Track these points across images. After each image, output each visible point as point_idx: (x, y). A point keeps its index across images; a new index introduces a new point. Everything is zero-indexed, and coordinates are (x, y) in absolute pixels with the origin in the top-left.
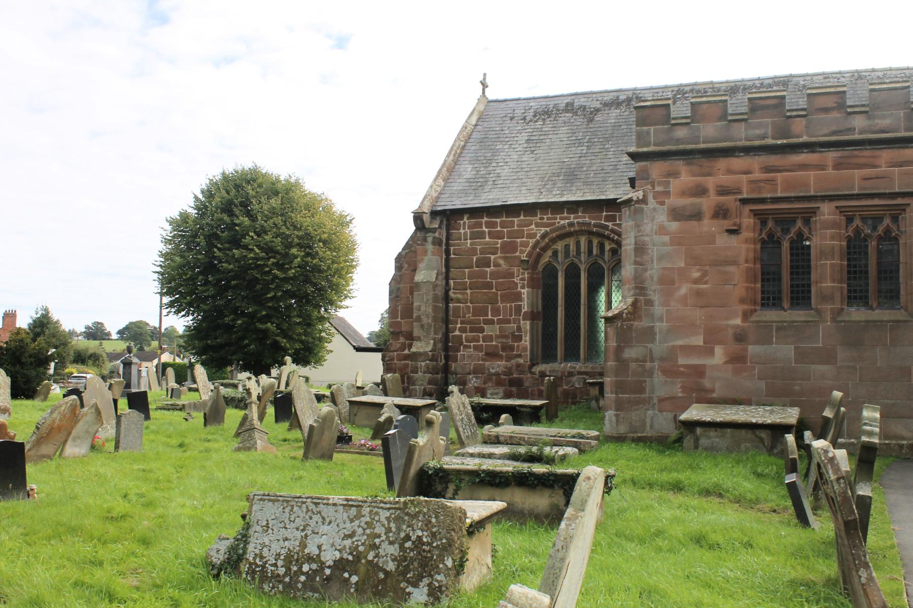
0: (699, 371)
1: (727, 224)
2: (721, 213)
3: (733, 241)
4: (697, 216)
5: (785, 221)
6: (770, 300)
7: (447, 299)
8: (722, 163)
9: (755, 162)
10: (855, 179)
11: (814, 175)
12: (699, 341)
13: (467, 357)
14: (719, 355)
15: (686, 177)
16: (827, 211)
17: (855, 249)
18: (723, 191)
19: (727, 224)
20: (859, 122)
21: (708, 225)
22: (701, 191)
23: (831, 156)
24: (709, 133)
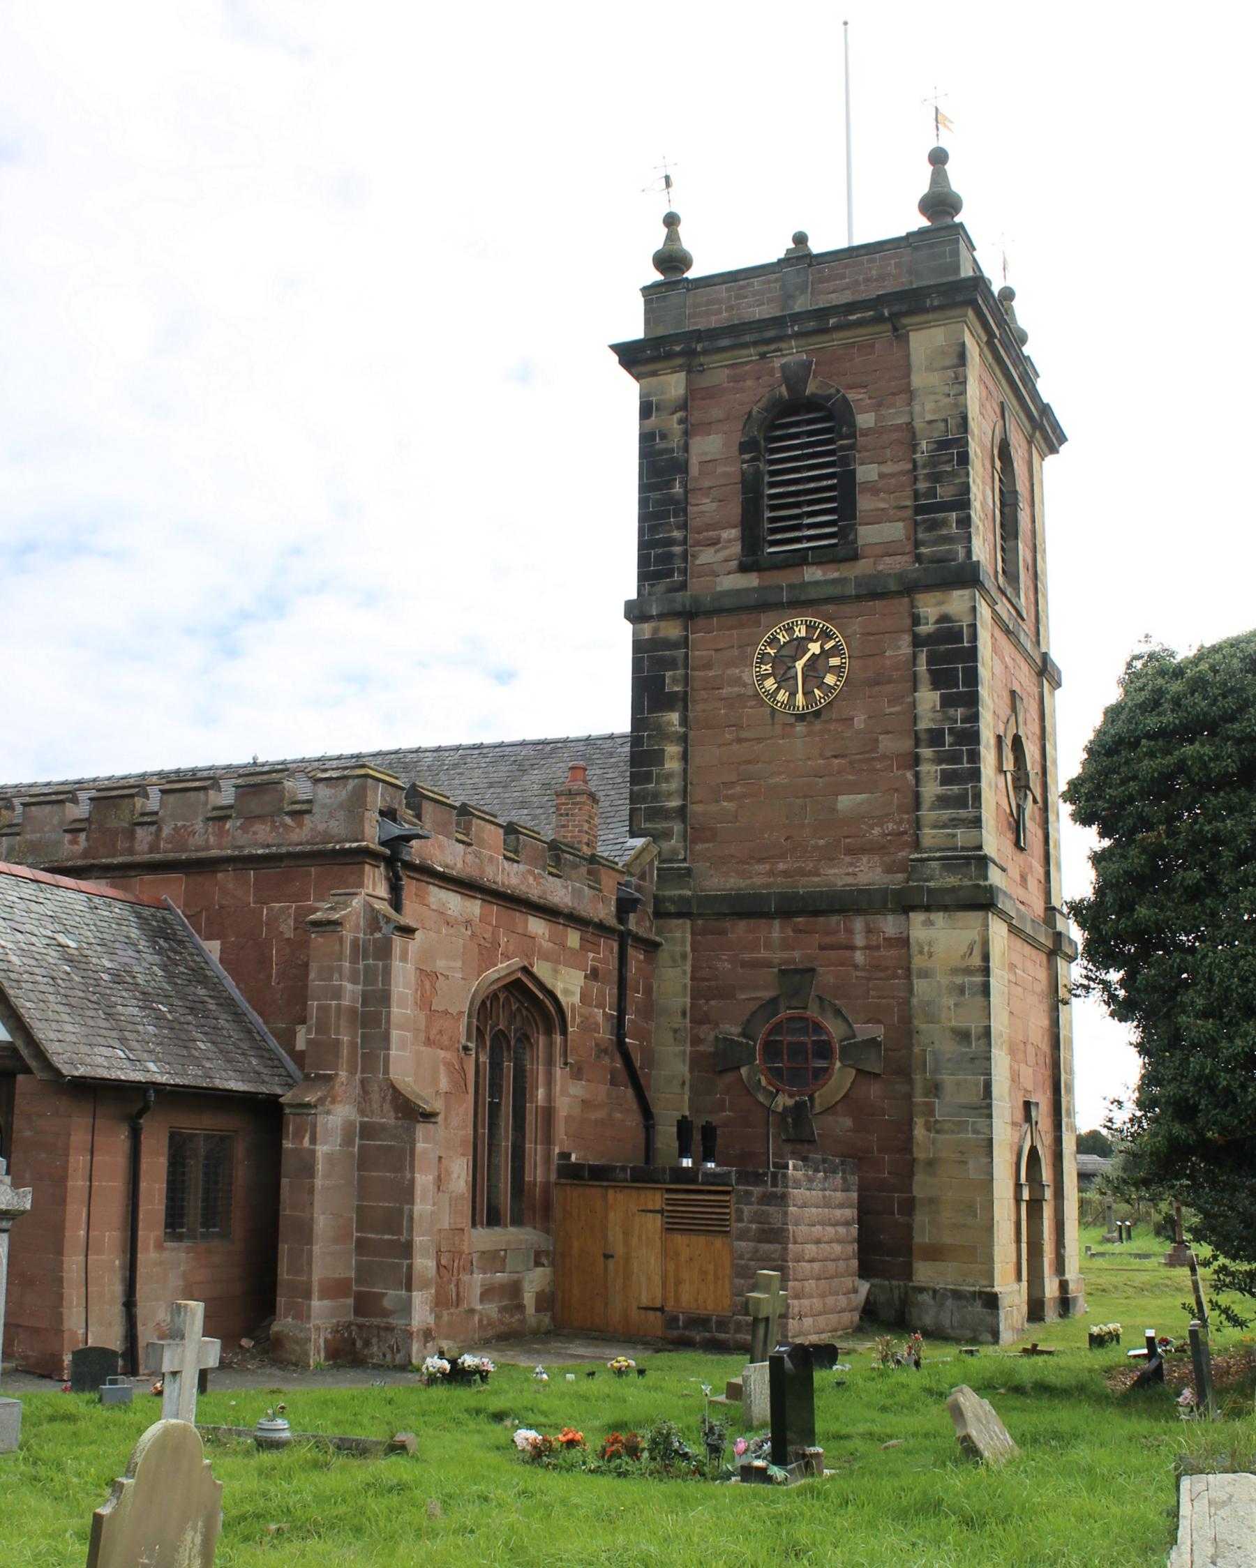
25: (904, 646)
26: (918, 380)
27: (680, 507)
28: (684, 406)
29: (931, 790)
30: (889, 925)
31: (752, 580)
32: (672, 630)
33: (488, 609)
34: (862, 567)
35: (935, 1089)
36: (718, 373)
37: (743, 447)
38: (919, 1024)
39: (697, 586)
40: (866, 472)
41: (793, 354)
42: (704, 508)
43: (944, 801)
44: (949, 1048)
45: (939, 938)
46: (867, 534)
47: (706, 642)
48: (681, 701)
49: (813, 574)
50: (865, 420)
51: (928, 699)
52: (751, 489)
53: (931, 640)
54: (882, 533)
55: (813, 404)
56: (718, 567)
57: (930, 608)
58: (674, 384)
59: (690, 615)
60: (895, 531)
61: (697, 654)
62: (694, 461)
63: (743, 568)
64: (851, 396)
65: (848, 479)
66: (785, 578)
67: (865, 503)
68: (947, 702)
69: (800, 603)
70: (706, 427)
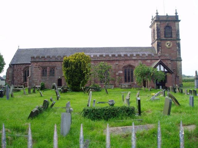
0: (37, 83)
1: (39, 68)
2: (39, 67)
3: (40, 70)
4: (36, 68)
5: (45, 68)
6: (43, 76)
7: (13, 75)
8: (39, 63)
9: (42, 63)
10: (51, 65)
11: (47, 64)
12: (36, 80)
13: (16, 81)
14: (38, 81)
15: (35, 64)
16: (48, 68)
17: (51, 71)
18: (39, 65)
19: (39, 68)
20: (51, 59)
21: (37, 69)
22: (37, 65)
23: (48, 62)
24: (37, 60)
25: (176, 44)
26: (176, 26)
27: (160, 32)
28: (160, 25)
29: (178, 53)
30: (175, 62)
31: (165, 38)
32: (160, 41)
33: (143, 38)
34: (172, 39)
35: (179, 72)
36: (162, 23)
37: (164, 29)
38: (178, 68)
39: (161, 38)
40: (173, 32)
41: (167, 23)
42: (161, 33)
43: (179, 54)
44: (179, 69)
45: (178, 63)
46: (173, 36)
47: (162, 42)
48: (161, 46)
49: (169, 38)
50: (172, 28)
51: (177, 47)
52: (165, 32)
53: (178, 44)
54: (174, 36)
55: (169, 26)
56: (163, 37)
57: (177, 41)
58: (159, 23)
59: (161, 40)
60: (175, 36)
61: (162, 43)
62: (161, 29)
63: (165, 37)
64: (172, 26)
65: (172, 32)
66: (167, 38)
67: (173, 34)
68: (179, 48)
69: (169, 40)
70: (161, 27)
